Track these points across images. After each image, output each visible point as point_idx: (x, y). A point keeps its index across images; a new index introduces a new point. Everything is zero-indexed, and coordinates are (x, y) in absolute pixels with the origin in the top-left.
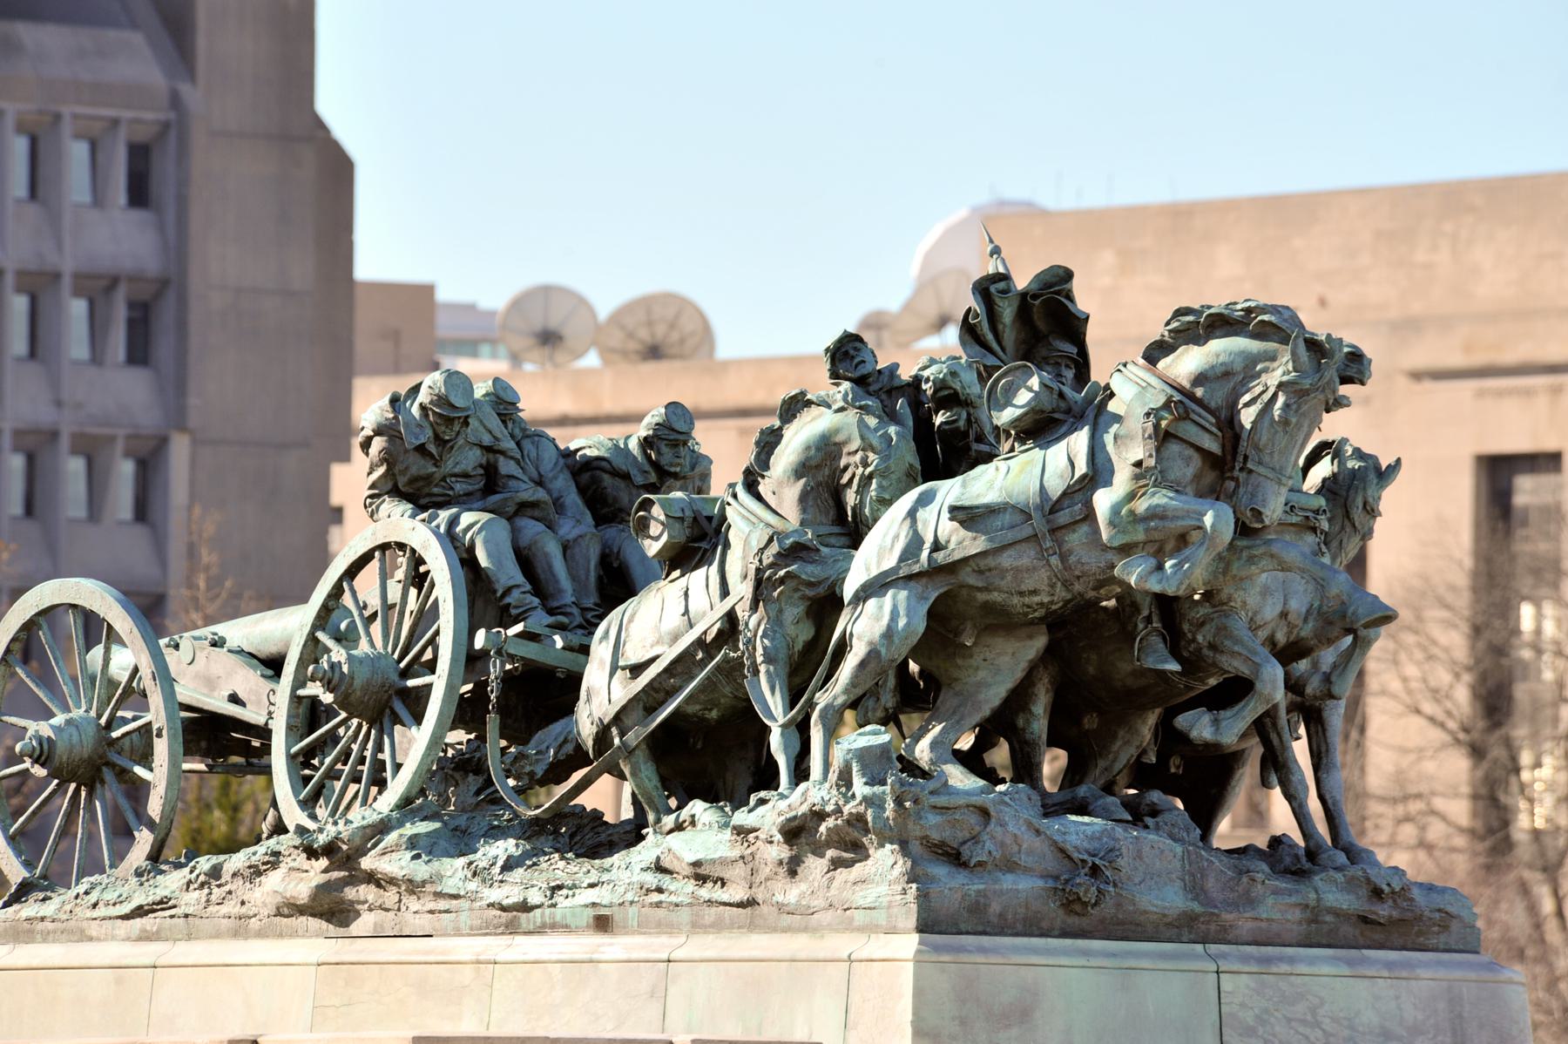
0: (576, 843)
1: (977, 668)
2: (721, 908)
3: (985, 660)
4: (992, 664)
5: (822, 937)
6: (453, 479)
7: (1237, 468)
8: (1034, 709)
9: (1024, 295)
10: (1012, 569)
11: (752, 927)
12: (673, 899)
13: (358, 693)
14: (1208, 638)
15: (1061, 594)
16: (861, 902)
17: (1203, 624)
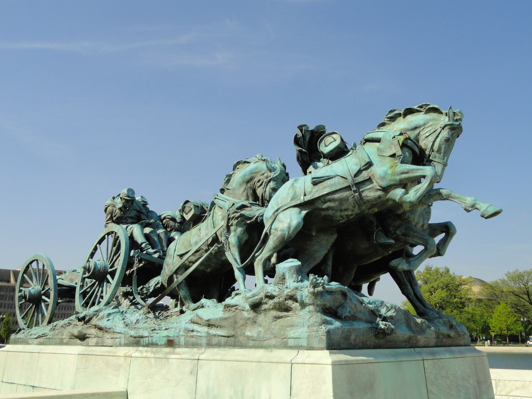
0: (160, 316)
1: (315, 245)
2: (220, 338)
3: (317, 242)
4: (320, 244)
5: (272, 351)
6: (129, 218)
7: (425, 160)
8: (328, 263)
9: (312, 131)
10: (339, 200)
11: (235, 345)
12: (199, 334)
13: (97, 273)
14: (402, 232)
15: (357, 211)
16: (292, 335)
17: (399, 227)
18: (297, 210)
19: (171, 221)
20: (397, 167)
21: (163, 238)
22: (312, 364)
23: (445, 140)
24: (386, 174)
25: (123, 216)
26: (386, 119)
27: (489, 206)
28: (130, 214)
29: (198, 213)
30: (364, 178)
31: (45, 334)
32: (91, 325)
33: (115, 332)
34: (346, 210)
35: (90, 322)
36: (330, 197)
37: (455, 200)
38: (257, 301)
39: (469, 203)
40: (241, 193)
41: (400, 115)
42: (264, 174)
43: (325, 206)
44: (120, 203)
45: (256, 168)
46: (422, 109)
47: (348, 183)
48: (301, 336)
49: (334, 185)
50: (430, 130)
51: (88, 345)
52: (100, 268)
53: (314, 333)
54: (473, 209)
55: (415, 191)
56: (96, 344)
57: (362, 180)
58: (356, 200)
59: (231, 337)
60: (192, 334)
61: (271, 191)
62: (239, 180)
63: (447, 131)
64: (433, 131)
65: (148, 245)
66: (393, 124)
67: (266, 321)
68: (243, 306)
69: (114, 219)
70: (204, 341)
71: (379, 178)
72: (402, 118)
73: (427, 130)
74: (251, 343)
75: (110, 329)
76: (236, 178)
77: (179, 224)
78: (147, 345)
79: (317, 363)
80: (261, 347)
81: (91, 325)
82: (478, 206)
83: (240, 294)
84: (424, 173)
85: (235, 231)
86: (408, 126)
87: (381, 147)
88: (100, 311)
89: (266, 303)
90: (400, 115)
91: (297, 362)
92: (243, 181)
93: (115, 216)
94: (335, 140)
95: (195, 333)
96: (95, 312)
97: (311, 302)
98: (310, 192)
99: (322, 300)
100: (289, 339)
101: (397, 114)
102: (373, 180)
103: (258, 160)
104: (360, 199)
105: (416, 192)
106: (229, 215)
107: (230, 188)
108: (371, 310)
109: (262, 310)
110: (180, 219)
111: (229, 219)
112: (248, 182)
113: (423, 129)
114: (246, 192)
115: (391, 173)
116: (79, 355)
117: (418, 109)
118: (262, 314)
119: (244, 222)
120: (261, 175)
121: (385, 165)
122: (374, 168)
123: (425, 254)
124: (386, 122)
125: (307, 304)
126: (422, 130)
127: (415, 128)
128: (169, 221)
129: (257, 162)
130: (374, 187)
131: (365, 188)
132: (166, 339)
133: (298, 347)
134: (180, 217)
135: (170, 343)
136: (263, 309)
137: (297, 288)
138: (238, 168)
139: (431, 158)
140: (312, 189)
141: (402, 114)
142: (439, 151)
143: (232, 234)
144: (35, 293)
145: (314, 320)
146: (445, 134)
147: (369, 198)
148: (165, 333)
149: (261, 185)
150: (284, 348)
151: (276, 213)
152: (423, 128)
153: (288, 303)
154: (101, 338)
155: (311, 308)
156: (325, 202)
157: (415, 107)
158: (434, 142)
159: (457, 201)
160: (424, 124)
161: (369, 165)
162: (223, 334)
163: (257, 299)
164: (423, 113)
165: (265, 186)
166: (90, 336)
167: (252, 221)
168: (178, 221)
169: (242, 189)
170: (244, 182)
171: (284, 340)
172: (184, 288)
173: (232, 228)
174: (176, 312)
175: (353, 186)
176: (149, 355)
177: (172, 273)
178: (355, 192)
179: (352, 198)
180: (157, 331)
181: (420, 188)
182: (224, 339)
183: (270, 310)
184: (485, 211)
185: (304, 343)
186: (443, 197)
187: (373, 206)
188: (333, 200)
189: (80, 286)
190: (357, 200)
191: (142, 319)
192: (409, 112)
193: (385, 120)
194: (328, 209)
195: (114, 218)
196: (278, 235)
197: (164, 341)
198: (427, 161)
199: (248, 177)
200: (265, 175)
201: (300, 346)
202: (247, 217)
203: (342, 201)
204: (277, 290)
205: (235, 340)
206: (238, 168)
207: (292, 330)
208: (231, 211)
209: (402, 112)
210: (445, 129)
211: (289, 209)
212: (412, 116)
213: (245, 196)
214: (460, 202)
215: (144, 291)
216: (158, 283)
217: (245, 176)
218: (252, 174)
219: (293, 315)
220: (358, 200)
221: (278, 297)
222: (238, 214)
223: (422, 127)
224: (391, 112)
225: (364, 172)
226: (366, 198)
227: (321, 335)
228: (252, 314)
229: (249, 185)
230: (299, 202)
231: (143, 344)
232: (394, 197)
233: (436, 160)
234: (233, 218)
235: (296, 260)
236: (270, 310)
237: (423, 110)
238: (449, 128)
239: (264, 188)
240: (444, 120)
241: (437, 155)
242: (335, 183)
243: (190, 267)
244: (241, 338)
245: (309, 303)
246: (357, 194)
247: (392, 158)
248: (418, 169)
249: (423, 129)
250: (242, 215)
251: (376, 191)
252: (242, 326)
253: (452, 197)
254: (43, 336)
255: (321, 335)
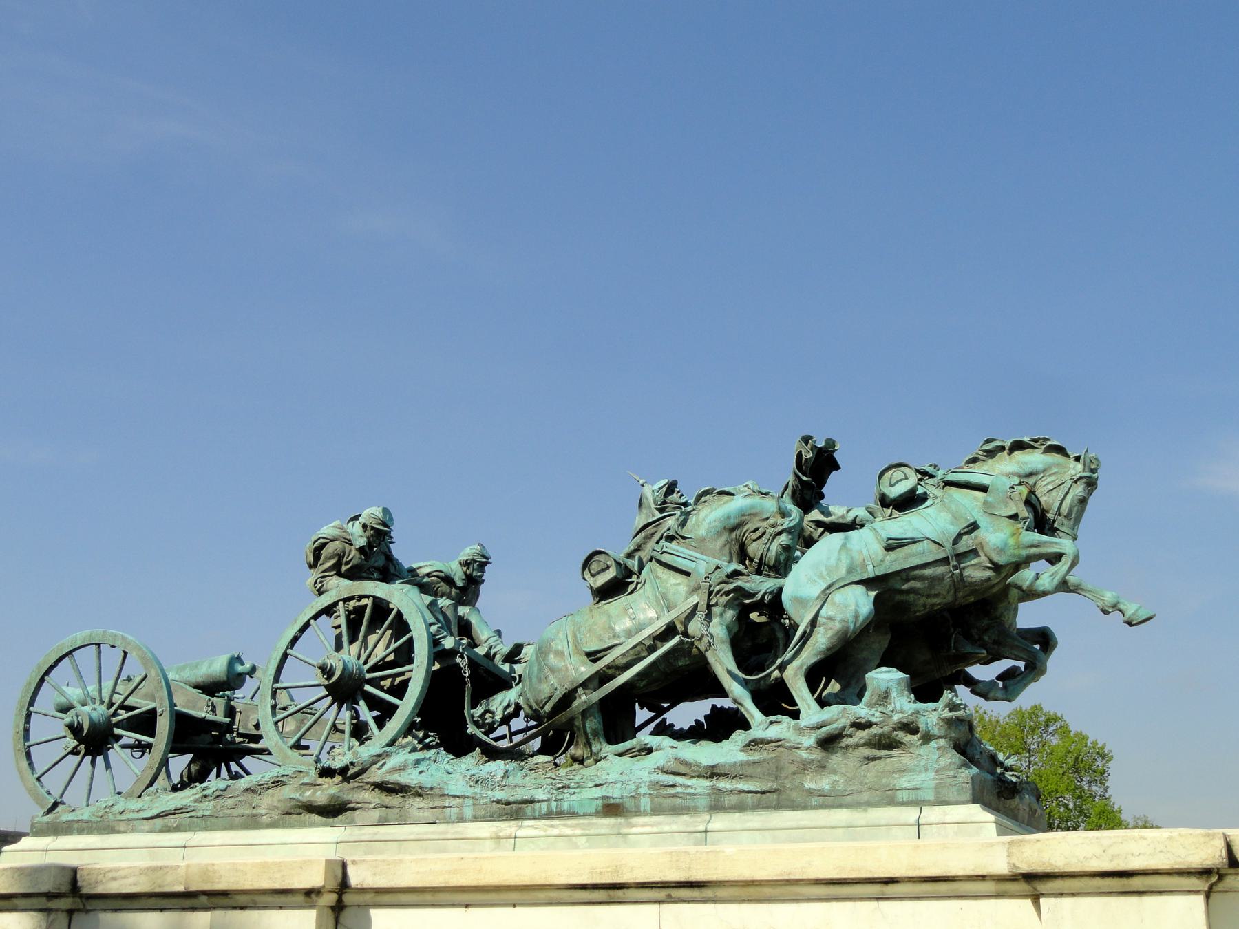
2: (743, 795)
5: (866, 811)
11: (778, 806)
12: (692, 791)
14: (993, 637)
15: (950, 598)
16: (905, 785)
17: (987, 630)
18: (860, 589)
19: (442, 583)
20: (1021, 536)
21: (451, 618)
22: (958, 823)
23: (1079, 500)
24: (1006, 544)
25: (363, 565)
26: (981, 453)
27: (1140, 607)
28: (376, 561)
29: (620, 577)
30: (967, 547)
31: (186, 809)
32: (361, 784)
33: (447, 795)
34: (936, 595)
35: (360, 777)
36: (917, 572)
37: (1086, 595)
38: (837, 732)
39: (1110, 600)
40: (718, 547)
41: (1002, 448)
42: (767, 519)
43: (905, 587)
44: (362, 536)
45: (752, 507)
46: (1036, 445)
47: (946, 553)
48: (924, 785)
49: (923, 553)
50: (1053, 481)
51: (352, 824)
52: (353, 671)
53: (949, 780)
54: (1114, 609)
55: (1051, 576)
56: (379, 822)
57: (964, 551)
58: (954, 582)
59: (769, 792)
60: (672, 791)
61: (780, 549)
62: (714, 524)
63: (1082, 486)
64: (1060, 483)
65: (442, 631)
66: (991, 461)
67: (846, 764)
68: (796, 742)
69: (344, 568)
70: (703, 802)
71: (994, 550)
72: (1005, 453)
73: (1049, 480)
74: (816, 801)
75: (432, 789)
76: (704, 520)
77: (458, 591)
78: (548, 816)
79: (969, 821)
80: (840, 806)
81: (361, 784)
82: (1122, 607)
83: (779, 722)
84: (1061, 549)
85: (721, 615)
86: (1020, 470)
87: (990, 499)
88: (387, 755)
89: (851, 736)
90: (1002, 448)
91: (929, 822)
92: (725, 527)
93: (347, 563)
94: (906, 478)
95: (678, 790)
96: (375, 758)
97: (942, 733)
98: (881, 561)
99: (958, 731)
100: (899, 791)
101: (997, 446)
102: (981, 553)
103: (751, 492)
104: (961, 580)
105: (1052, 578)
106: (710, 586)
107: (690, 536)
108: (991, 755)
109: (841, 747)
110: (463, 580)
111: (710, 593)
112: (733, 529)
113: (1043, 477)
114: (728, 546)
115: (1014, 544)
116: (337, 843)
117: (1032, 443)
118: (839, 754)
119: (739, 601)
120: (760, 520)
121: (1002, 530)
122: (982, 532)
123: (1032, 676)
124: (980, 456)
125: (935, 735)
126: (1041, 479)
127: (1031, 474)
128: (438, 583)
129: (750, 495)
130: (982, 562)
131: (968, 564)
132: (600, 803)
133: (919, 803)
134: (464, 577)
135: (611, 809)
136: (843, 744)
137: (918, 712)
138: (705, 502)
139: (1055, 526)
140: (885, 556)
141: (1007, 448)
142: (1068, 516)
143: (716, 620)
144: (100, 721)
145: (949, 761)
146: (1079, 490)
147: (973, 580)
148: (598, 793)
149: (760, 537)
150: (889, 805)
151: (828, 592)
152: (1042, 475)
153: (897, 735)
154: (398, 810)
155: (942, 742)
156: (908, 580)
157: (1026, 439)
158: (1062, 501)
159: (1090, 596)
160: (1044, 471)
161: (974, 527)
162: (751, 788)
163: (836, 728)
164: (1041, 451)
165: (770, 541)
166: (359, 805)
167: (755, 599)
168: (459, 583)
169: (722, 540)
170: (724, 528)
171: (887, 793)
172: (597, 715)
173: (716, 610)
174: (546, 763)
175: (952, 559)
176: (568, 831)
177: (575, 685)
178: (956, 568)
179: (949, 577)
180: (571, 791)
181: (1056, 571)
182: (752, 796)
183: (857, 746)
184: (1133, 614)
185: (930, 795)
186: (1068, 587)
187: (973, 592)
188: (921, 578)
189: (271, 706)
190: (956, 580)
191: (514, 769)
192: (1018, 446)
193: (980, 454)
194: (908, 592)
195: (343, 566)
196: (835, 629)
197: (597, 805)
198: (1049, 529)
199: (733, 521)
200: (771, 521)
201: (921, 801)
202: (747, 592)
203: (934, 580)
204: (877, 714)
205: (779, 798)
206: (705, 502)
207: (903, 777)
208: (715, 578)
209: (1007, 444)
210: (1078, 483)
211: (850, 586)
212: (1023, 453)
213: (728, 555)
214: (1093, 598)
215: (486, 719)
216: (509, 706)
217: (729, 518)
218: (744, 515)
219: (902, 755)
220: (958, 581)
221: (881, 726)
222: (732, 586)
223: (1041, 473)
224: (988, 441)
225: (965, 537)
226: (969, 579)
227: (963, 783)
228: (818, 755)
229: (734, 535)
230: (866, 576)
231: (532, 815)
232: (1019, 583)
233: (1064, 529)
234: (718, 592)
235: (895, 669)
236: (857, 746)
237: (1040, 447)
238: (1085, 483)
239: (766, 544)
240: (1077, 469)
241: (1066, 522)
242: (924, 550)
243: (616, 677)
244: (794, 795)
245: (938, 735)
246: (958, 571)
247: (1010, 520)
248: (1052, 543)
249: (1043, 477)
250: (738, 589)
251: (984, 570)
252: (794, 774)
253: (1082, 590)
254: (177, 811)
255: (963, 783)
